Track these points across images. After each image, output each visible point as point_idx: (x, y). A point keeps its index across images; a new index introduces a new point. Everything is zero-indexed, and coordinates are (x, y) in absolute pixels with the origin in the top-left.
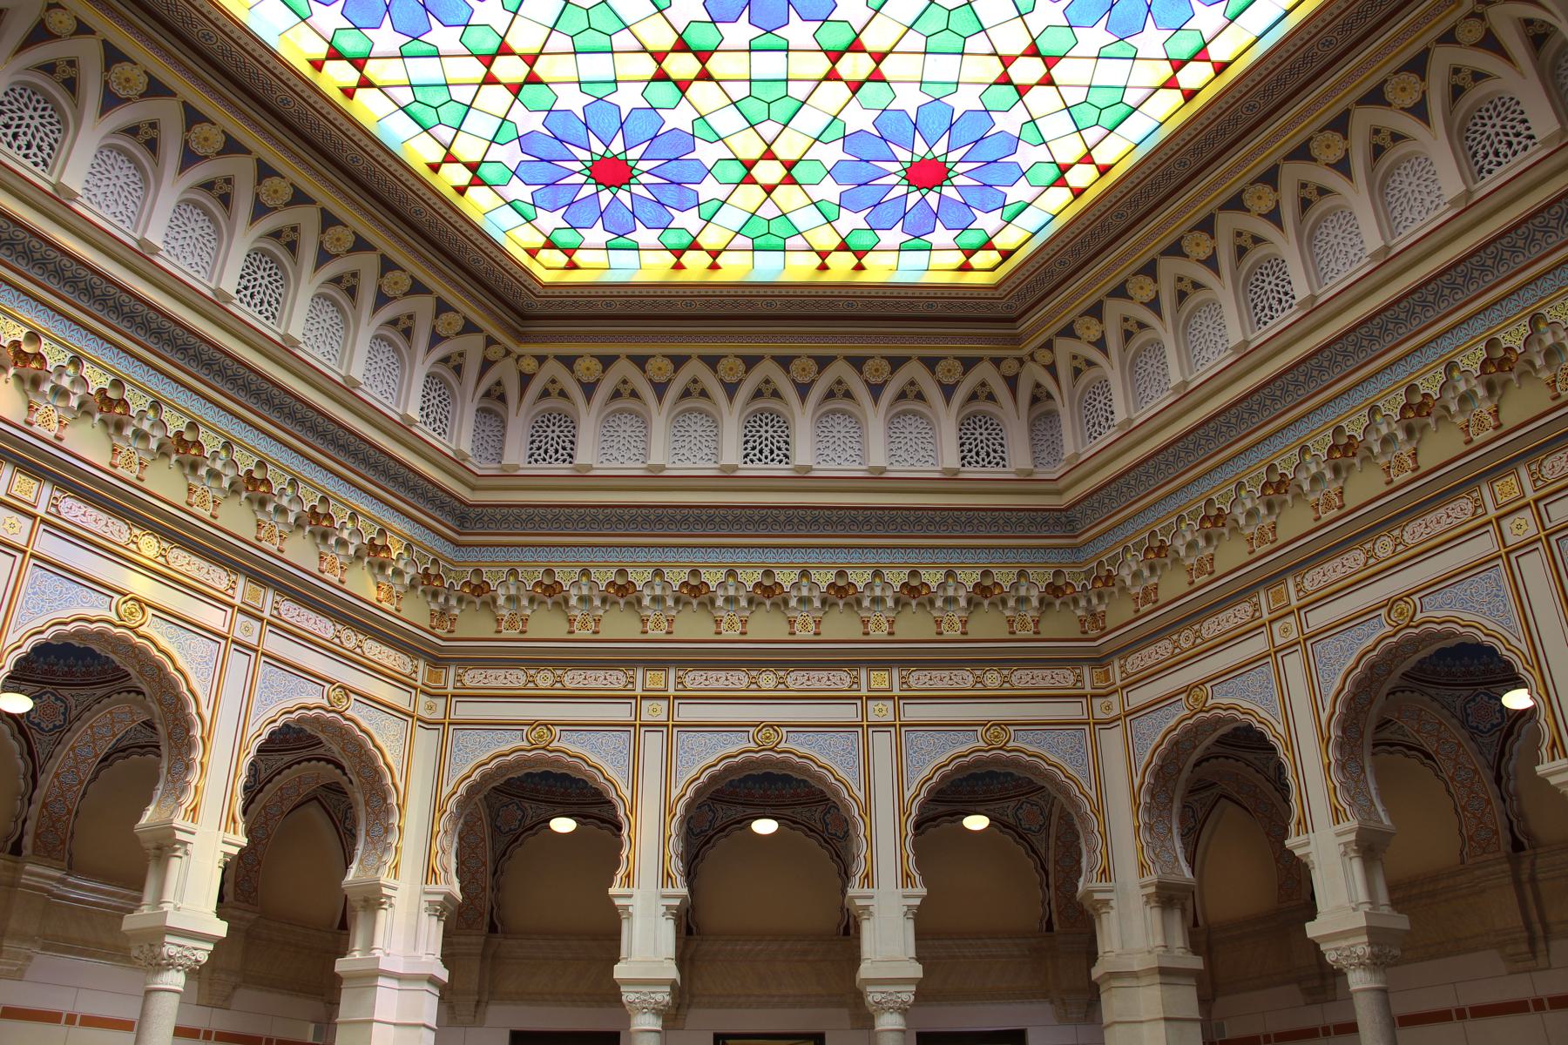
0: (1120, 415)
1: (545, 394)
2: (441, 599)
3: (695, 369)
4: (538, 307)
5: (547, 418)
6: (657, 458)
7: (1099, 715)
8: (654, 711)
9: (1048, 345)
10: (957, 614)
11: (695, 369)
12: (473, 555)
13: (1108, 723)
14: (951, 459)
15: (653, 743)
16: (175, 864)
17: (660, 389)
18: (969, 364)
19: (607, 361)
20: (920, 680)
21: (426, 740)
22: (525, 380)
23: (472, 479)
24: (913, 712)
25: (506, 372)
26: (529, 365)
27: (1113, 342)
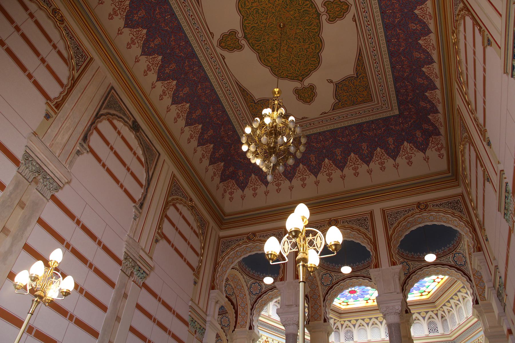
0: (457, 323)
1: (346, 327)
3: (374, 320)
4: (343, 312)
5: (347, 332)
6: (369, 339)
9: (442, 307)
11: (374, 320)
14: (426, 332)
17: (368, 324)
18: (427, 312)
19: (357, 320)
22: (342, 325)
25: (338, 324)
26: (342, 322)
27: (454, 307)
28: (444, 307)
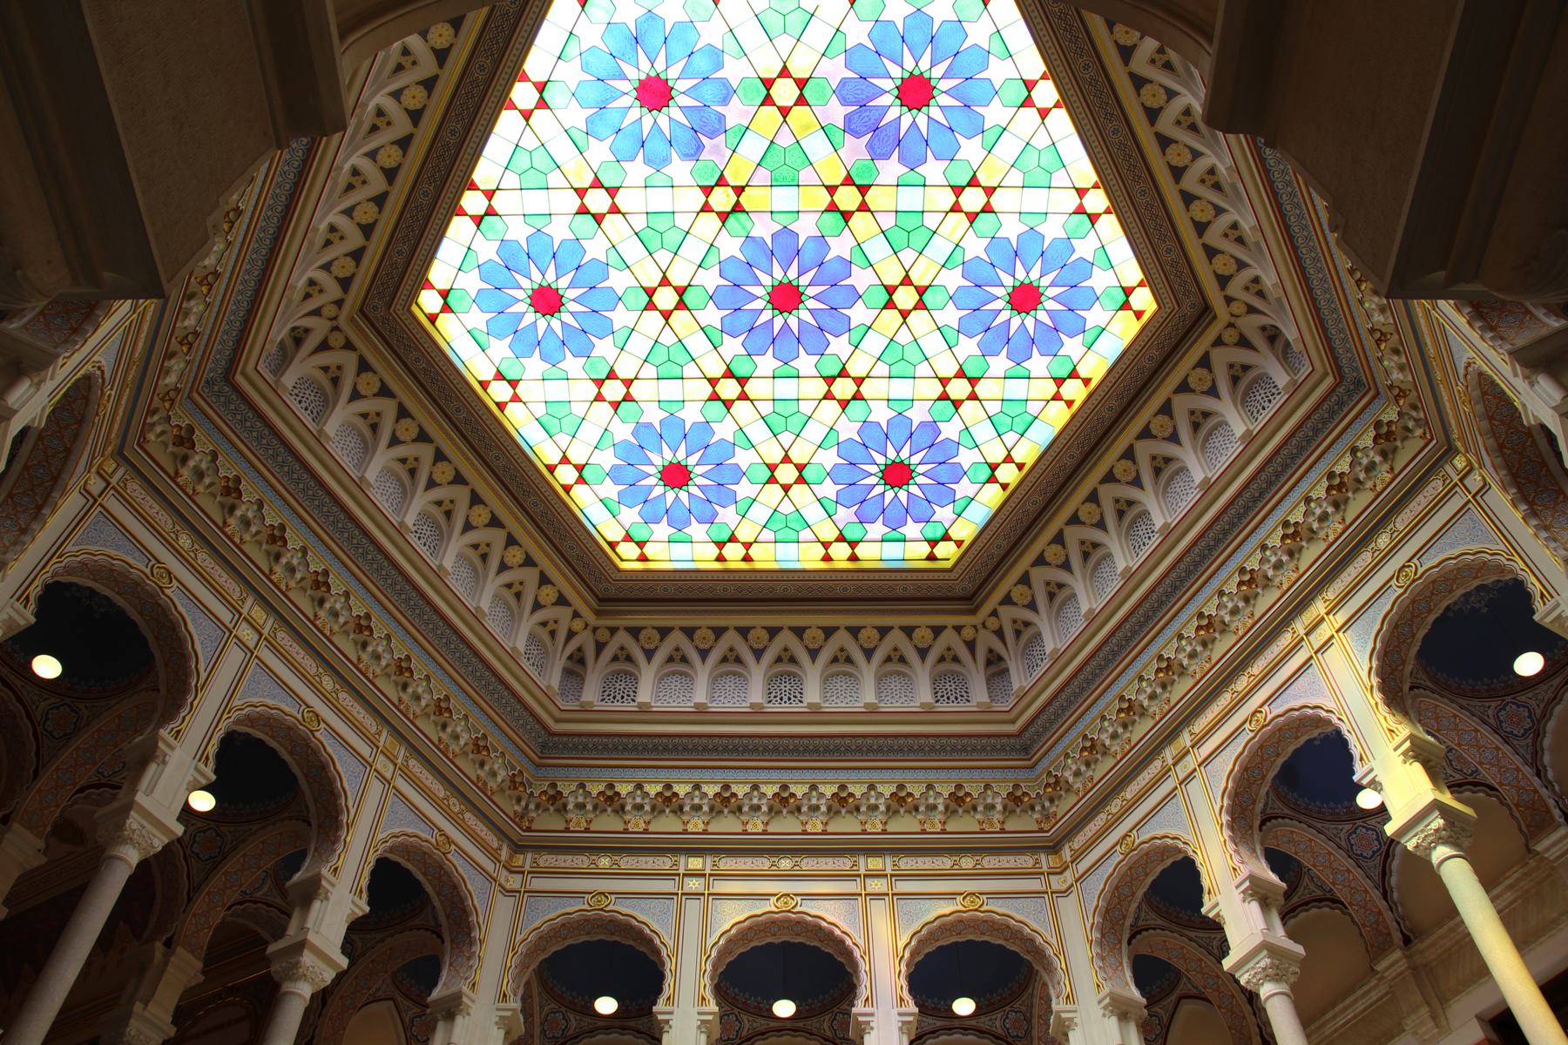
2: (523, 803)
7: (1055, 887)
8: (693, 885)
10: (938, 817)
12: (551, 772)
13: (1066, 892)
15: (693, 907)
16: (317, 905)
20: (907, 863)
21: (504, 905)
23: (557, 713)
24: (902, 886)
26: (603, 635)
28: (1003, 610)
